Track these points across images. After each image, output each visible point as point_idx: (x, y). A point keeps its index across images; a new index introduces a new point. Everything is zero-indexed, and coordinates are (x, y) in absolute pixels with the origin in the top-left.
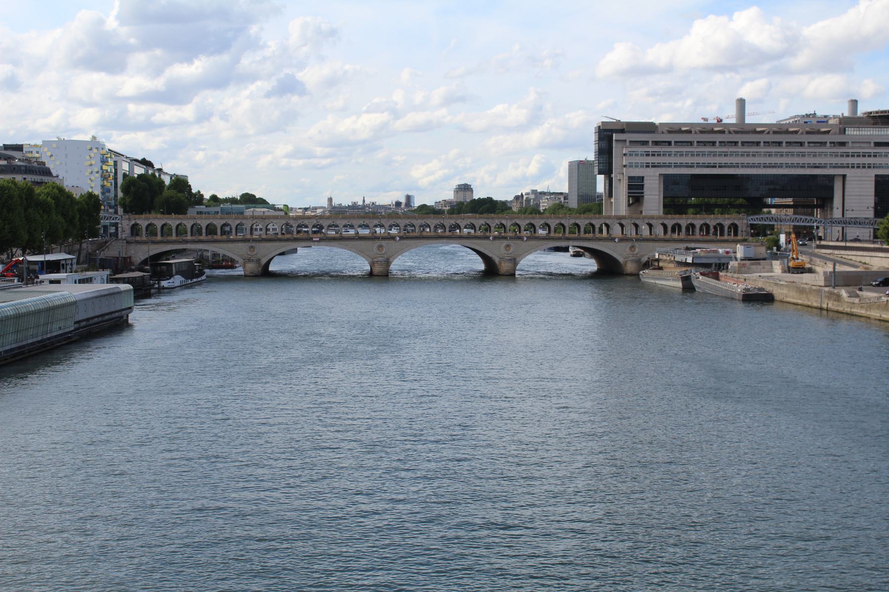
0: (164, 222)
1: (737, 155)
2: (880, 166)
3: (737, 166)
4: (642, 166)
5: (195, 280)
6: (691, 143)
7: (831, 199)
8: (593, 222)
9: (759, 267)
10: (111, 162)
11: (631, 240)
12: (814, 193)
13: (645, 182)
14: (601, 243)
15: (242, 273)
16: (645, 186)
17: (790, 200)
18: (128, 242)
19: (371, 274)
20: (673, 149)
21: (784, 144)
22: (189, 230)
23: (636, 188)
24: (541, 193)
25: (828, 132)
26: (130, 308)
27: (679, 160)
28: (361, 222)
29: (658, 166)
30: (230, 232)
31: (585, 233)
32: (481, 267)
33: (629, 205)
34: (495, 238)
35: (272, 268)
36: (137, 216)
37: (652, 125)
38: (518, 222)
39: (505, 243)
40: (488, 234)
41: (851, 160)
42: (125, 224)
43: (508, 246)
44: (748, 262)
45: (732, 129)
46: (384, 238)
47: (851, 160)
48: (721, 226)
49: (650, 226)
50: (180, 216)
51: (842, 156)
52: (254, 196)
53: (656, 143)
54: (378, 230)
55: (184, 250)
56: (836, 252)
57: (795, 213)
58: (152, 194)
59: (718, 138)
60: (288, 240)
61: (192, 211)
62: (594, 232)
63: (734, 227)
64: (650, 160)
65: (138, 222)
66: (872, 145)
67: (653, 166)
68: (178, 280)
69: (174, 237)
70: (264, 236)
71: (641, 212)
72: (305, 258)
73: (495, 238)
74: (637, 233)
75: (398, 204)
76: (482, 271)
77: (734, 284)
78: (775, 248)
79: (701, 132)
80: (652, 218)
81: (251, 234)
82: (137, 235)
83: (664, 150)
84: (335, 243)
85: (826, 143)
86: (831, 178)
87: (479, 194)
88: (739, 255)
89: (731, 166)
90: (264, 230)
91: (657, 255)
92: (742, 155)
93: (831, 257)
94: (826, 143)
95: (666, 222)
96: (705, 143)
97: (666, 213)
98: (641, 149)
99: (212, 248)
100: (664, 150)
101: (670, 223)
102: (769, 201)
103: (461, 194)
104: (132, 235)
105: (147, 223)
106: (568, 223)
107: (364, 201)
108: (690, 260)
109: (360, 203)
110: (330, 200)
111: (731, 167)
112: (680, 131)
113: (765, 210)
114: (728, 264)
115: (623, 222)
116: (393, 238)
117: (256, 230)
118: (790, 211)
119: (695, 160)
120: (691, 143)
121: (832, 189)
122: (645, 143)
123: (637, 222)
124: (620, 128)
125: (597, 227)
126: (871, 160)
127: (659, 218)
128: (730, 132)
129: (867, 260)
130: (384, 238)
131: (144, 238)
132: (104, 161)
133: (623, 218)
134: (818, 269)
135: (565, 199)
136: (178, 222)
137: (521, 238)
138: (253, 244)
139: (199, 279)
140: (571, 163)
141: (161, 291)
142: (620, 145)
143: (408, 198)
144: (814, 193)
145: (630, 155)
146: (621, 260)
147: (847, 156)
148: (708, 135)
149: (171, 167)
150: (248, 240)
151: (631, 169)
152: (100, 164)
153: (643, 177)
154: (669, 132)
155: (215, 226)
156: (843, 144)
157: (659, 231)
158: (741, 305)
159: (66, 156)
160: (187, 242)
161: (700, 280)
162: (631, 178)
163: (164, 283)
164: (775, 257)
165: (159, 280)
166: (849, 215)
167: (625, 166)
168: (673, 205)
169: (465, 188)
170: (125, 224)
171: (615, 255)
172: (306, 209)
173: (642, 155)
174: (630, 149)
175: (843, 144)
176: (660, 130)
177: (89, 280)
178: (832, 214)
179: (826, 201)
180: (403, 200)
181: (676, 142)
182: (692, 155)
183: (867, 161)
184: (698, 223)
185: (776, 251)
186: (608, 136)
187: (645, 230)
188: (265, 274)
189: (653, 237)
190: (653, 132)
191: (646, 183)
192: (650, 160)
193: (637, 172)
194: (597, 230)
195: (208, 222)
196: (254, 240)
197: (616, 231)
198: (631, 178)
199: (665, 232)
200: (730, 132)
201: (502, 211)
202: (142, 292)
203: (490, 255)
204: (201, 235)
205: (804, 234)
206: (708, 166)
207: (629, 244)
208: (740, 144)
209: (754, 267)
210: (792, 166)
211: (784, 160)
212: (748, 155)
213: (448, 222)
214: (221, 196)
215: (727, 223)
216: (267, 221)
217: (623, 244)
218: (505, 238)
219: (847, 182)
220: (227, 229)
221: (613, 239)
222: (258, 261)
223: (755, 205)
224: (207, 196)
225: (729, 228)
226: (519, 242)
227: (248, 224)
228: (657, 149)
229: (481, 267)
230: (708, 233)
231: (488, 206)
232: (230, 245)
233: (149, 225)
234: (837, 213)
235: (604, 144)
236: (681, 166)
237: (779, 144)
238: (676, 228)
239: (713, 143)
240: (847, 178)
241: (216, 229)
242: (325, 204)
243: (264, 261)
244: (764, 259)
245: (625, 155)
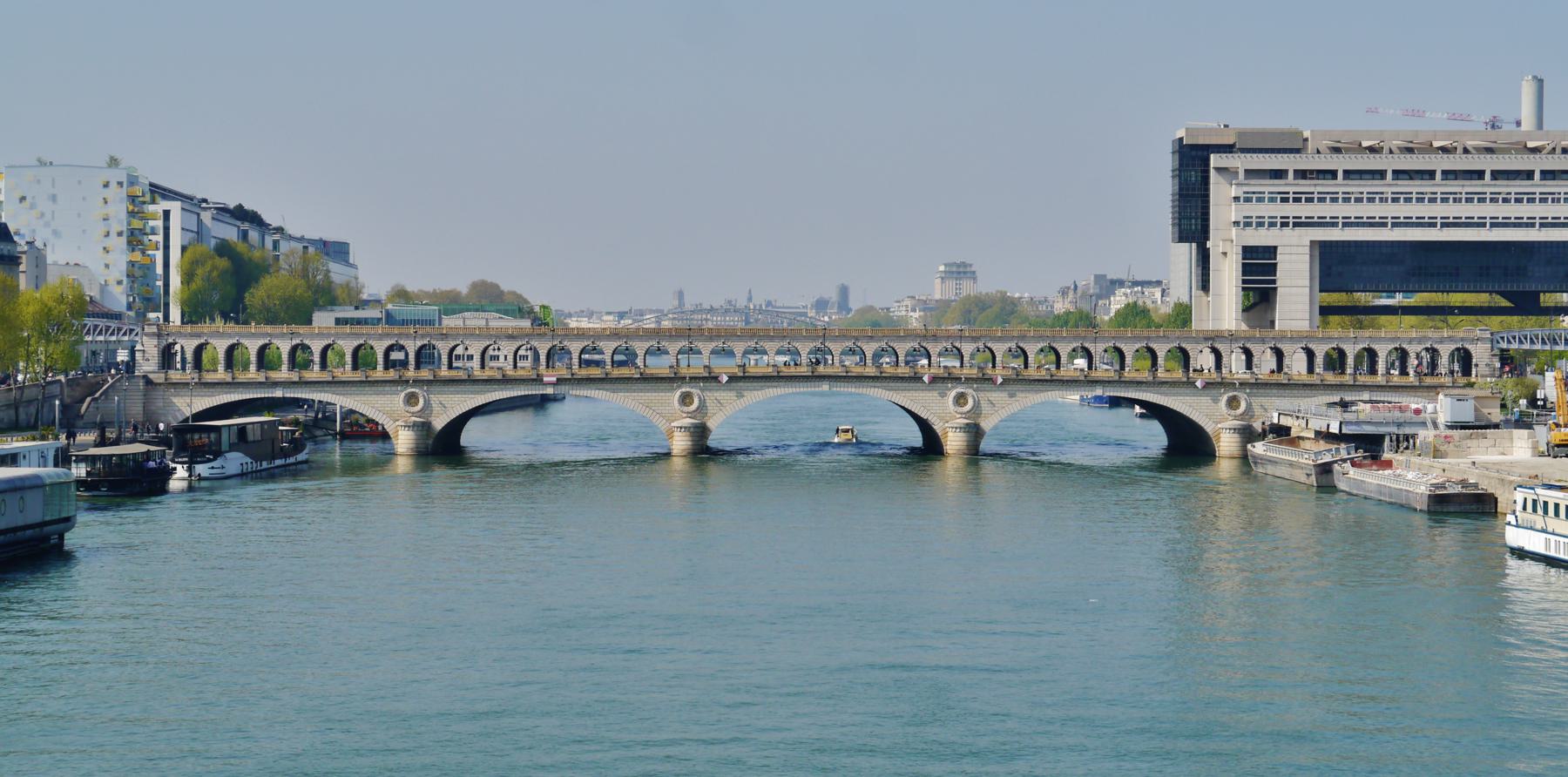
5: (278, 462)
11: (1229, 385)
20: (1339, 186)
22: (285, 357)
23: (1259, 267)
24: (1113, 282)
26: (67, 519)
27: (1352, 210)
30: (404, 364)
32: (916, 438)
35: (471, 436)
44: (1457, 433)
45: (1470, 143)
49: (1279, 354)
52: (497, 286)
55: (297, 400)
59: (1441, 163)
64: (1291, 210)
67: (1295, 225)
69: (221, 374)
71: (1273, 323)
72: (586, 419)
75: (821, 305)
77: (1412, 477)
80: (1283, 337)
81: (450, 367)
87: (986, 285)
91: (1276, 415)
97: (1325, 324)
98: (1269, 187)
99: (341, 401)
102: (1547, 299)
103: (952, 284)
107: (750, 299)
108: (1334, 429)
112: (1360, 149)
114: (1414, 436)
115: (1218, 346)
117: (496, 358)
128: (1466, 151)
139: (292, 460)
143: (844, 292)
145: (1248, 200)
146: (1209, 428)
153: (1275, 248)
157: (1297, 365)
160: (276, 384)
161: (1354, 477)
162: (1248, 251)
164: (1523, 423)
169: (960, 271)
172: (621, 315)
173: (1272, 200)
180: (833, 295)
185: (1532, 413)
186: (1193, 162)
187: (1265, 363)
190: (1298, 151)
192: (1291, 210)
198: (1248, 251)
199: (1311, 370)
200: (1466, 151)
201: (1125, 319)
202: (132, 483)
203: (924, 415)
206: (1420, 224)
209: (1474, 443)
220: (396, 356)
224: (464, 289)
225: (1358, 357)
228: (1305, 186)
229: (916, 438)
231: (1006, 309)
233: (360, 346)
235: (1194, 176)
238: (1336, 361)
241: (374, 354)
242: (670, 303)
244: (1496, 426)
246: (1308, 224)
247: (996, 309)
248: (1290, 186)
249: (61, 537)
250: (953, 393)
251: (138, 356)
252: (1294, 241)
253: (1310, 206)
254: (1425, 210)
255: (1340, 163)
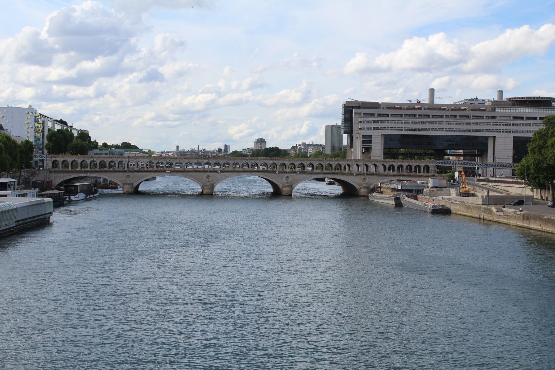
0: (73, 159)
1: (429, 123)
2: (516, 132)
3: (429, 130)
4: (371, 129)
5: (92, 196)
6: (401, 115)
7: (486, 151)
8: (340, 163)
9: (442, 192)
10: (41, 122)
11: (363, 174)
12: (476, 147)
13: (373, 139)
14: (345, 176)
15: (122, 192)
16: (373, 141)
17: (462, 151)
18: (50, 172)
19: (202, 195)
20: (390, 119)
21: (458, 117)
22: (89, 164)
23: (367, 143)
24: (308, 145)
25: (485, 110)
26: (51, 213)
27: (393, 126)
28: (196, 161)
29: (381, 129)
31: (335, 170)
32: (271, 190)
33: (363, 153)
34: (280, 172)
35: (140, 189)
36: (56, 155)
37: (377, 103)
38: (294, 162)
39: (285, 175)
40: (275, 170)
41: (498, 127)
42: (49, 161)
43: (287, 177)
45: (426, 107)
46: (210, 171)
47: (498, 127)
48: (419, 167)
49: (376, 166)
50: (84, 156)
51: (493, 125)
52: (130, 144)
53: (380, 115)
54: (207, 166)
55: (86, 177)
56: (489, 184)
57: (464, 160)
58: (66, 142)
60: (150, 172)
61: (91, 153)
62: (341, 169)
63: (427, 168)
64: (376, 125)
65: (57, 159)
66: (512, 118)
68: (81, 196)
70: (136, 169)
71: (370, 157)
72: (161, 183)
73: (280, 172)
74: (367, 170)
75: (220, 150)
76: (271, 193)
77: (426, 202)
78: (452, 181)
79: (407, 109)
80: (377, 161)
81: (128, 167)
82: (56, 167)
83: (384, 119)
84: (181, 174)
85: (483, 116)
86: (487, 138)
87: (270, 145)
88: (430, 185)
89: (426, 130)
90: (136, 165)
92: (432, 123)
93: (486, 186)
94: (483, 116)
95: (385, 164)
96: (409, 116)
97: (385, 158)
99: (103, 176)
100: (384, 119)
101: (387, 164)
103: (259, 144)
104: (53, 167)
105: (62, 160)
106: (325, 163)
107: (198, 148)
108: (399, 187)
109: (196, 149)
110: (177, 147)
111: (425, 130)
112: (394, 108)
113: (446, 157)
114: (423, 190)
115: (359, 163)
116: (216, 171)
117: (131, 165)
118: (462, 158)
119: (404, 126)
120: (401, 115)
121: (487, 145)
122: (373, 115)
123: (367, 163)
124: (357, 105)
125: (343, 166)
126: (511, 128)
127: (381, 161)
128: (425, 109)
129: (508, 189)
130: (210, 171)
131: (61, 169)
132: (36, 121)
133: (359, 161)
134: (478, 194)
135: (323, 148)
136: (82, 159)
137: (295, 173)
138: (129, 174)
139: (95, 195)
140: (327, 126)
141: (70, 202)
142: (358, 116)
143: (226, 147)
144: (476, 147)
145: (364, 122)
147: (497, 125)
148: (412, 110)
149: (78, 125)
150: (126, 172)
151: (364, 131)
152: (34, 123)
154: (388, 108)
155: (105, 162)
156: (494, 117)
157: (381, 169)
158: (430, 215)
159: (13, 117)
160: (87, 172)
161: (406, 200)
162: (363, 136)
163: (73, 198)
164: (452, 186)
165: (69, 196)
166: (497, 161)
167: (360, 129)
168: (389, 153)
169: (261, 141)
170: (49, 161)
171: (353, 184)
172: (162, 153)
173: (371, 122)
174: (363, 119)
175: (494, 117)
176: (382, 107)
177: (25, 195)
178: (487, 160)
179: (483, 152)
180: (223, 148)
181: (391, 115)
182: (402, 123)
183: (508, 128)
184: (405, 165)
185: (452, 183)
186: (350, 110)
187: (372, 169)
188: (136, 193)
189: (377, 173)
190: (377, 108)
191: (373, 140)
192: (376, 125)
193: (368, 133)
194: (343, 168)
195: (101, 160)
196: (129, 172)
197: (355, 169)
199: (385, 170)
200: (425, 109)
201: (284, 155)
202: (59, 203)
203: (276, 182)
204: (96, 168)
205: (469, 172)
207: (362, 177)
208: (431, 116)
209: (439, 192)
210: (463, 130)
211: (458, 127)
212: (436, 123)
213: (251, 162)
214: (109, 144)
215: (422, 165)
216: (138, 160)
217: (359, 177)
218: (286, 172)
219: (496, 141)
220: (113, 164)
221: (352, 174)
222: (132, 184)
223: (440, 154)
224: (100, 144)
225: (424, 168)
226: (294, 175)
227: (125, 161)
228: (380, 119)
229: (271, 190)
230: (411, 171)
231: (276, 152)
232: (115, 174)
233: (64, 161)
234: (490, 160)
235: (348, 115)
236: (395, 129)
237: (455, 116)
238: (392, 167)
239: (415, 116)
240: (496, 139)
241: (106, 164)
242: (174, 149)
243: (135, 185)
244: (445, 188)
245: (360, 122)
246: (513, 132)
247: (275, 152)
248: (376, 119)
249: (49, 218)
250: (285, 176)
251: (45, 163)
252: (377, 134)
253: (381, 124)
254: (400, 126)
255: (390, 112)
